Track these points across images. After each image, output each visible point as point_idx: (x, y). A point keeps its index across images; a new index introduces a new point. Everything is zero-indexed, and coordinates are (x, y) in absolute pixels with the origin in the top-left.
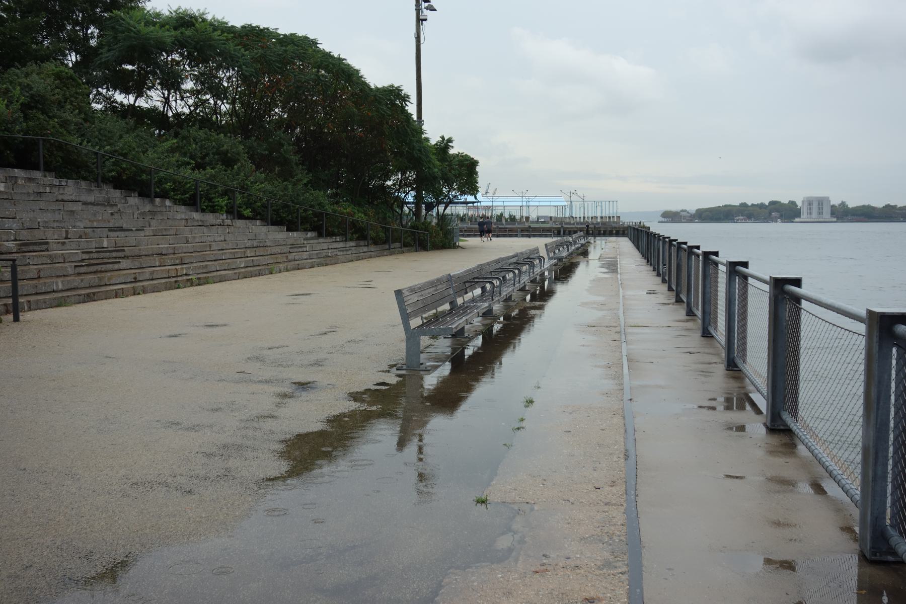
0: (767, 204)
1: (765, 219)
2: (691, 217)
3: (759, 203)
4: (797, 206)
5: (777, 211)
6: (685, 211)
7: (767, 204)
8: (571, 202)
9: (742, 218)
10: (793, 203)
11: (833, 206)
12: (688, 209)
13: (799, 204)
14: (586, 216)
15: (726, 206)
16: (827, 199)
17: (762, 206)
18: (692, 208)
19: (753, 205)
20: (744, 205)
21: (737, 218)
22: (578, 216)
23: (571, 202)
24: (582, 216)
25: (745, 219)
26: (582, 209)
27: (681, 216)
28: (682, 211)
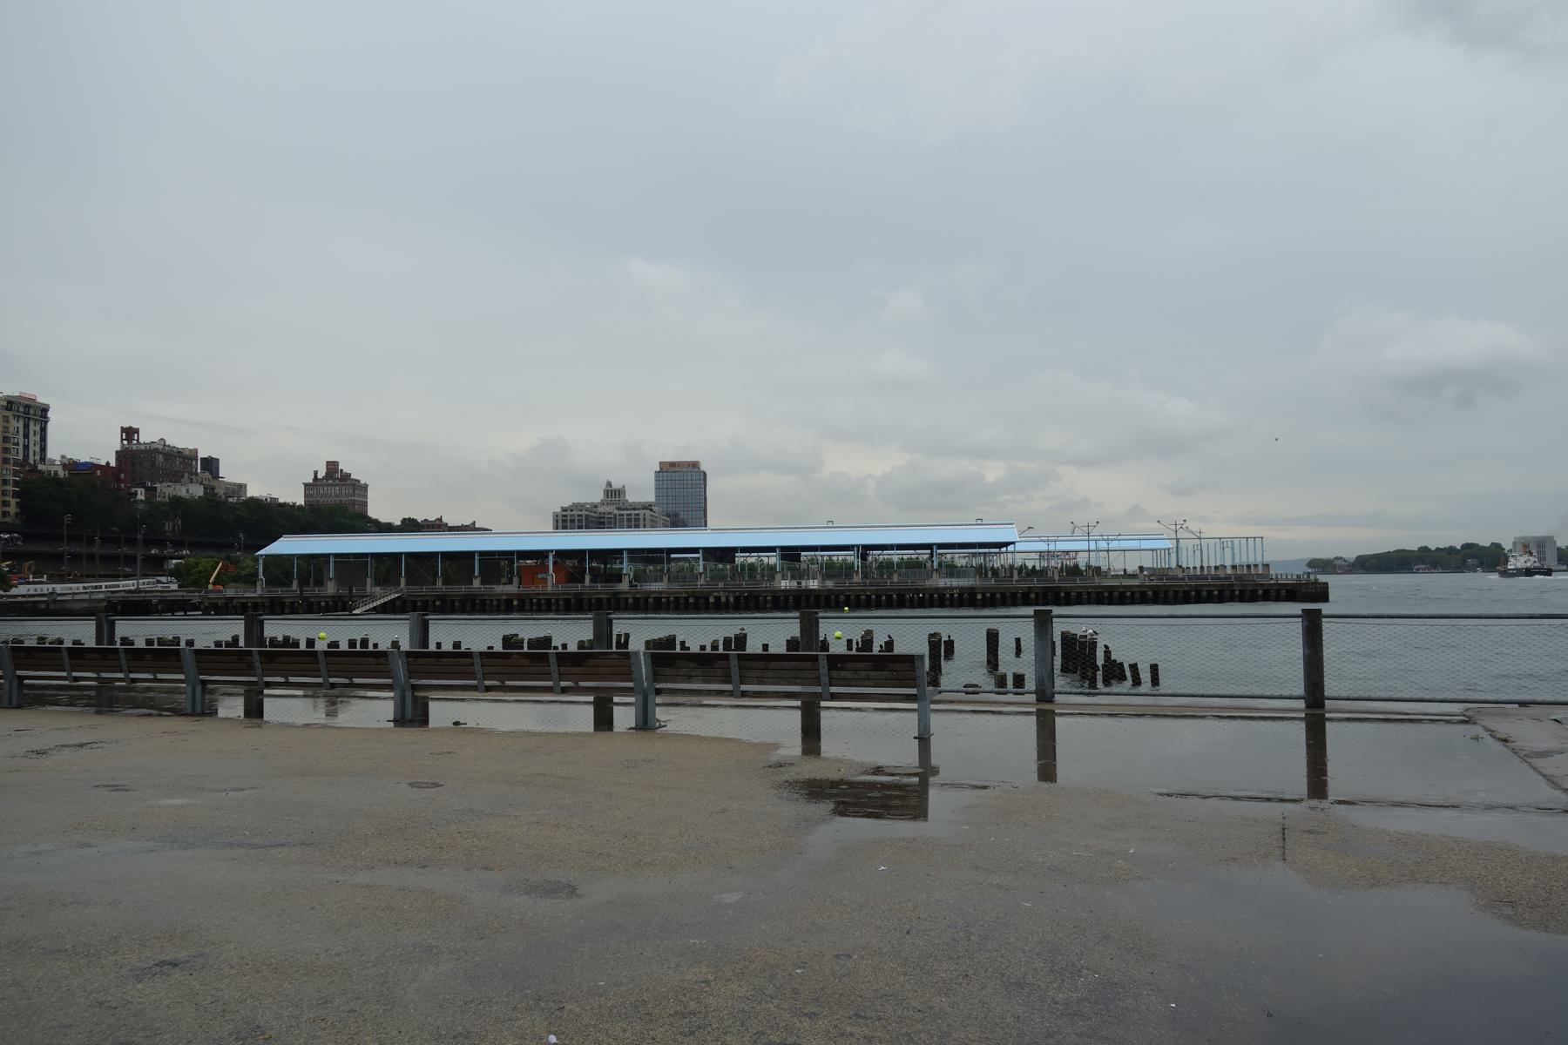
0: (1459, 548)
1: (1459, 568)
2: (1348, 566)
3: (1447, 546)
4: (1504, 549)
5: (1475, 557)
6: (1341, 558)
7: (1459, 548)
8: (1178, 540)
9: (1423, 566)
10: (1497, 546)
11: (1559, 549)
12: (1344, 556)
13: (1507, 546)
14: (1205, 565)
15: (1398, 551)
16: (1551, 540)
17: (1451, 550)
18: (1351, 555)
19: (1438, 549)
20: (1424, 549)
21: (1416, 567)
22: (1191, 566)
23: (1178, 540)
24: (1198, 566)
25: (1428, 568)
26: (1198, 553)
27: (1335, 566)
28: (1336, 558)
